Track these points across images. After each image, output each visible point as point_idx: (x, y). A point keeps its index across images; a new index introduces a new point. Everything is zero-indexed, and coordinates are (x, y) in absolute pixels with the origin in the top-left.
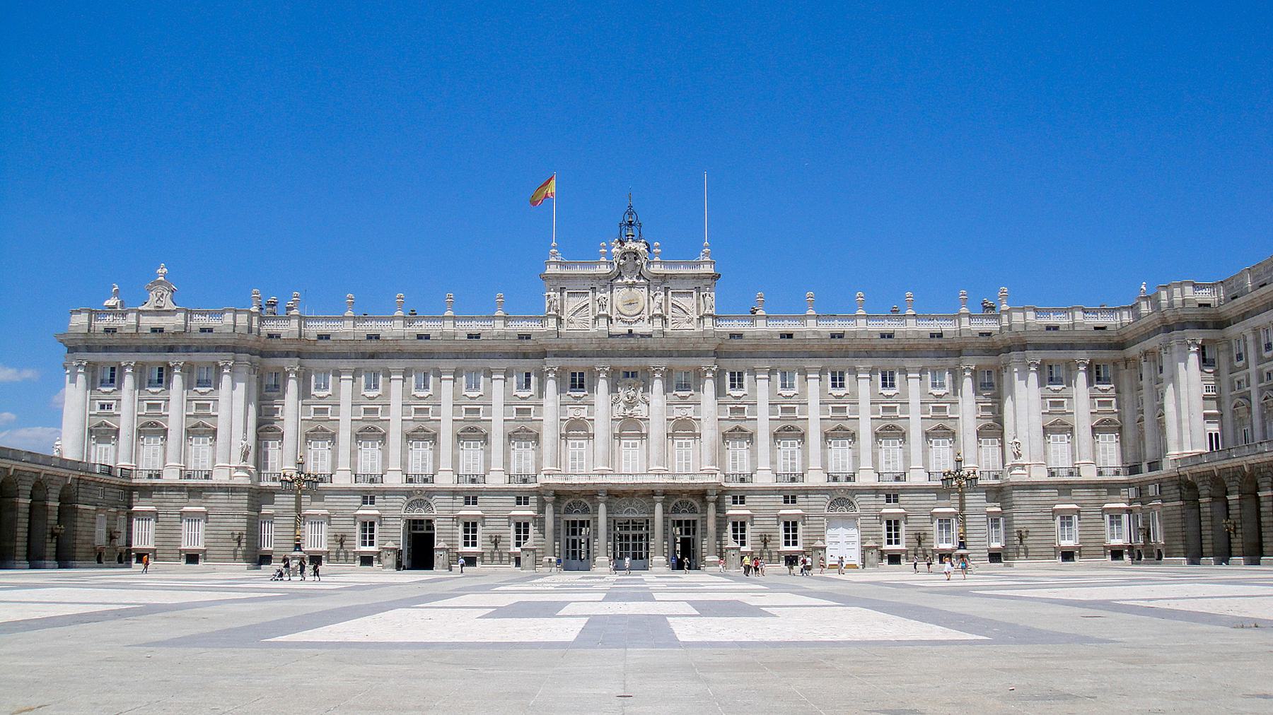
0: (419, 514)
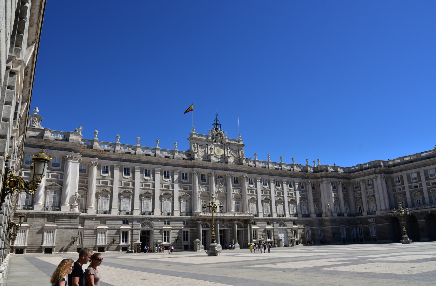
0: (146, 228)
